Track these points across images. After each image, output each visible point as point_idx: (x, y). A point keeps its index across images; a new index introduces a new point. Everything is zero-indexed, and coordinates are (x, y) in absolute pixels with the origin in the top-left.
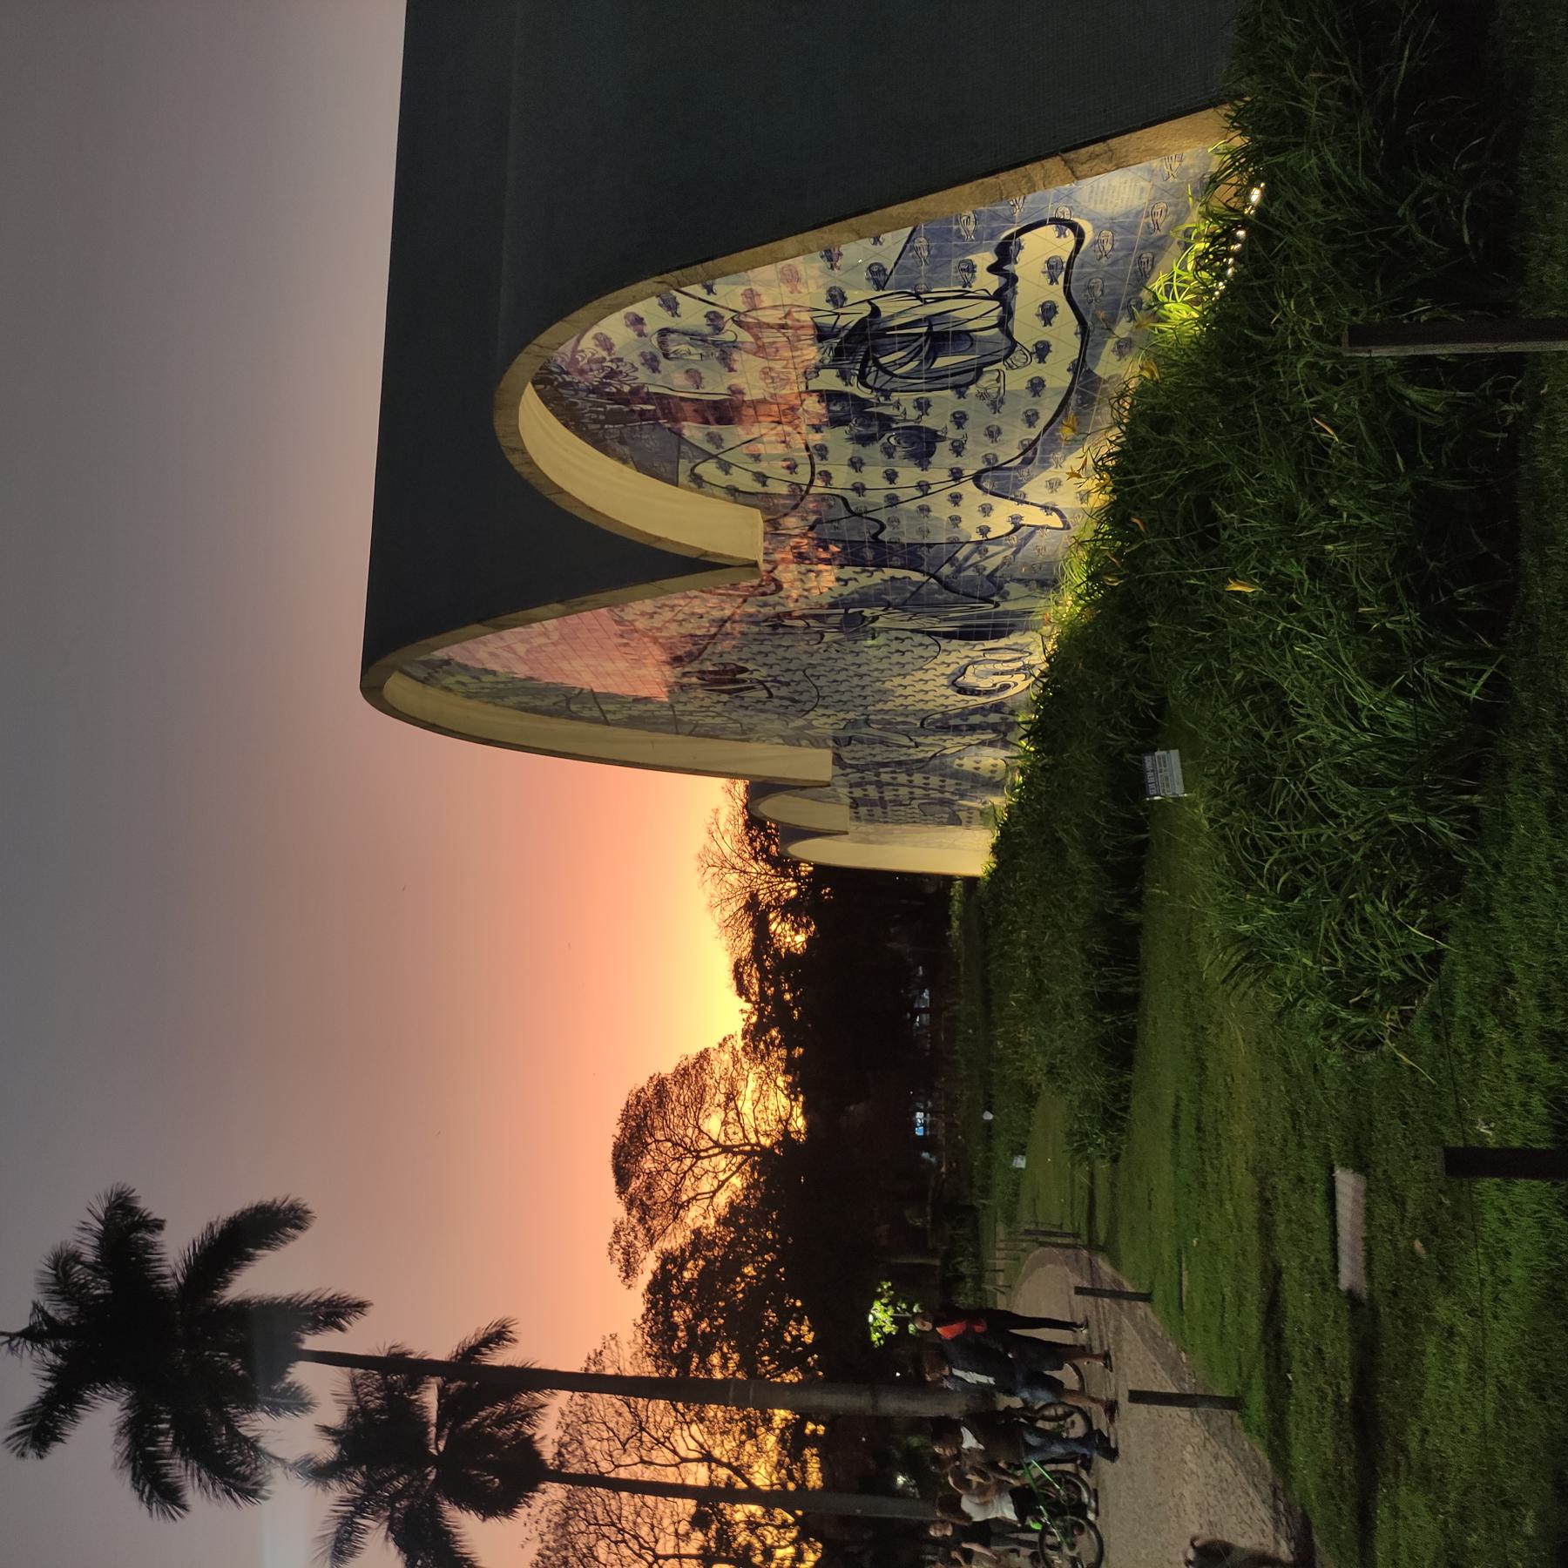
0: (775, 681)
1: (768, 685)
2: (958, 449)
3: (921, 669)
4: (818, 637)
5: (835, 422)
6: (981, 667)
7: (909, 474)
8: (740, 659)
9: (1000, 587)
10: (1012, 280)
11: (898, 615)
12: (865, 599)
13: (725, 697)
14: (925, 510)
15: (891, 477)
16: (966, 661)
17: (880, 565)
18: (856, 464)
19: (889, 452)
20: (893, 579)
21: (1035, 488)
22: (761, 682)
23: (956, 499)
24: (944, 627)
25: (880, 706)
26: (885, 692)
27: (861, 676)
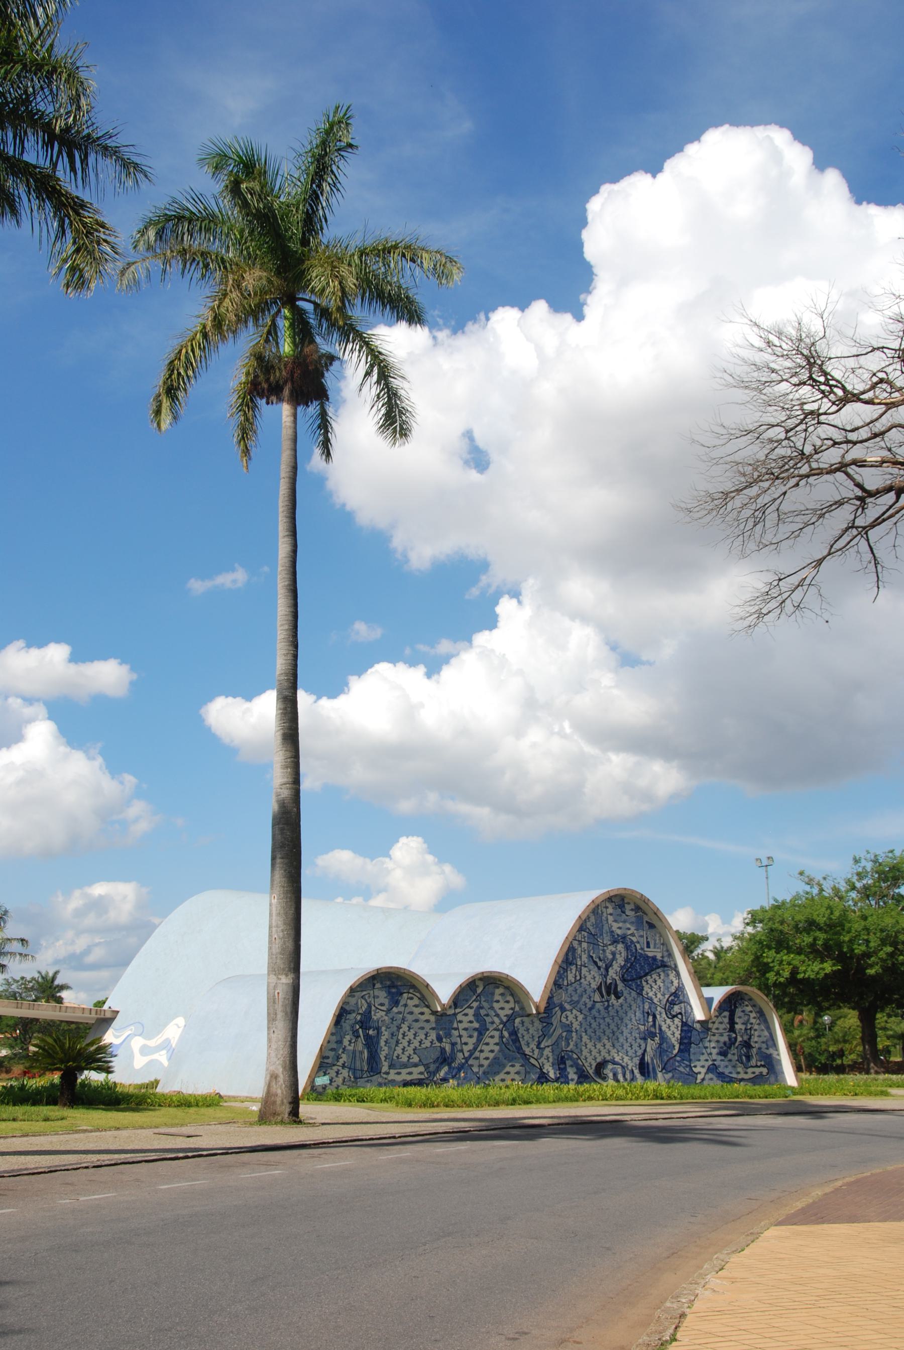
0: (608, 1006)
1: (606, 1003)
2: (722, 1060)
3: (618, 1051)
4: (642, 1023)
5: (730, 1039)
6: (620, 1070)
7: (715, 1051)
8: (626, 999)
9: (670, 1072)
10: (759, 1067)
11: (655, 1046)
12: (663, 1038)
13: (594, 985)
14: (703, 1054)
15: (714, 1048)
16: (623, 1064)
17: (680, 1044)
18: (718, 1041)
19: (721, 1048)
20: (674, 1046)
21: (710, 1075)
22: (608, 1001)
23: (707, 1060)
24: (647, 1058)
25: (585, 1038)
26: (599, 1039)
27: (613, 1033)
